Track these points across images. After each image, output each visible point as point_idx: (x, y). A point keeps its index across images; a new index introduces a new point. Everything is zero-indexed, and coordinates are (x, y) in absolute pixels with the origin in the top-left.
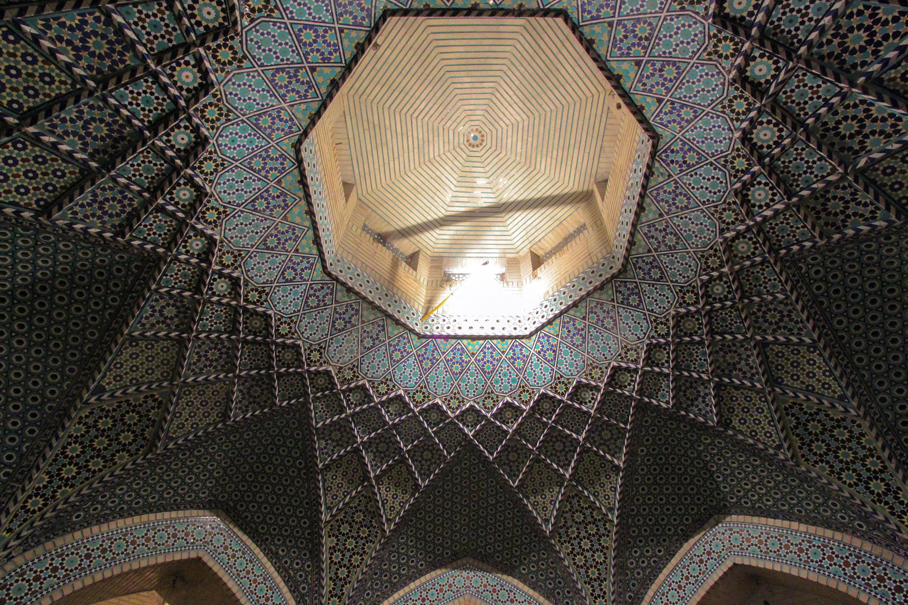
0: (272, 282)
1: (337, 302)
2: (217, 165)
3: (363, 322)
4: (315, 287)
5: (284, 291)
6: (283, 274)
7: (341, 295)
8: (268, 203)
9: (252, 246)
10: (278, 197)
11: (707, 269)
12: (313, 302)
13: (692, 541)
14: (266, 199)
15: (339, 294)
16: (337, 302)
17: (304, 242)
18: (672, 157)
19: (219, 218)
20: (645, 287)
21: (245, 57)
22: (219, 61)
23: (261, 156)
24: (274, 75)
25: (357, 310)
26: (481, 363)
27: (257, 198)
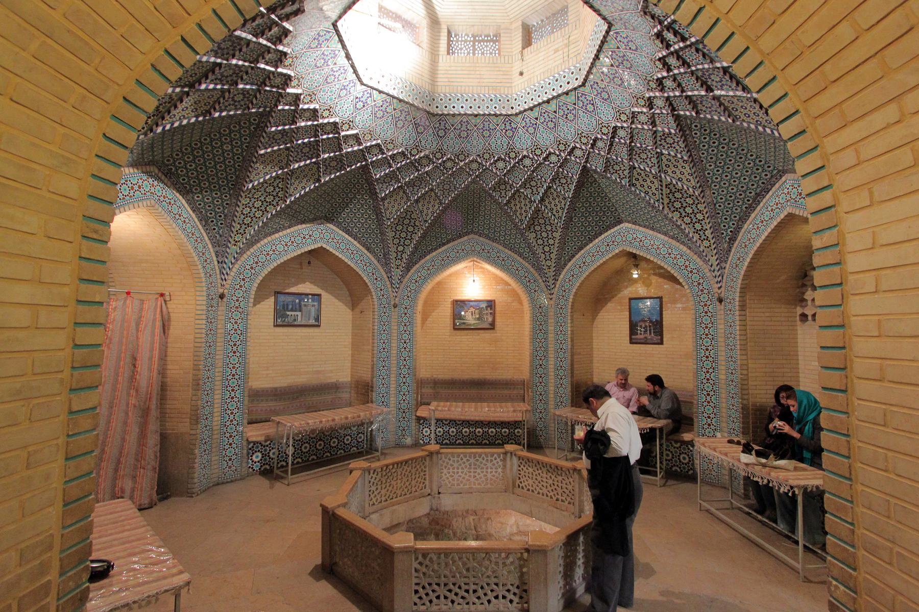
11: (457, 156)
13: (304, 226)
18: (508, 124)
20: (431, 131)
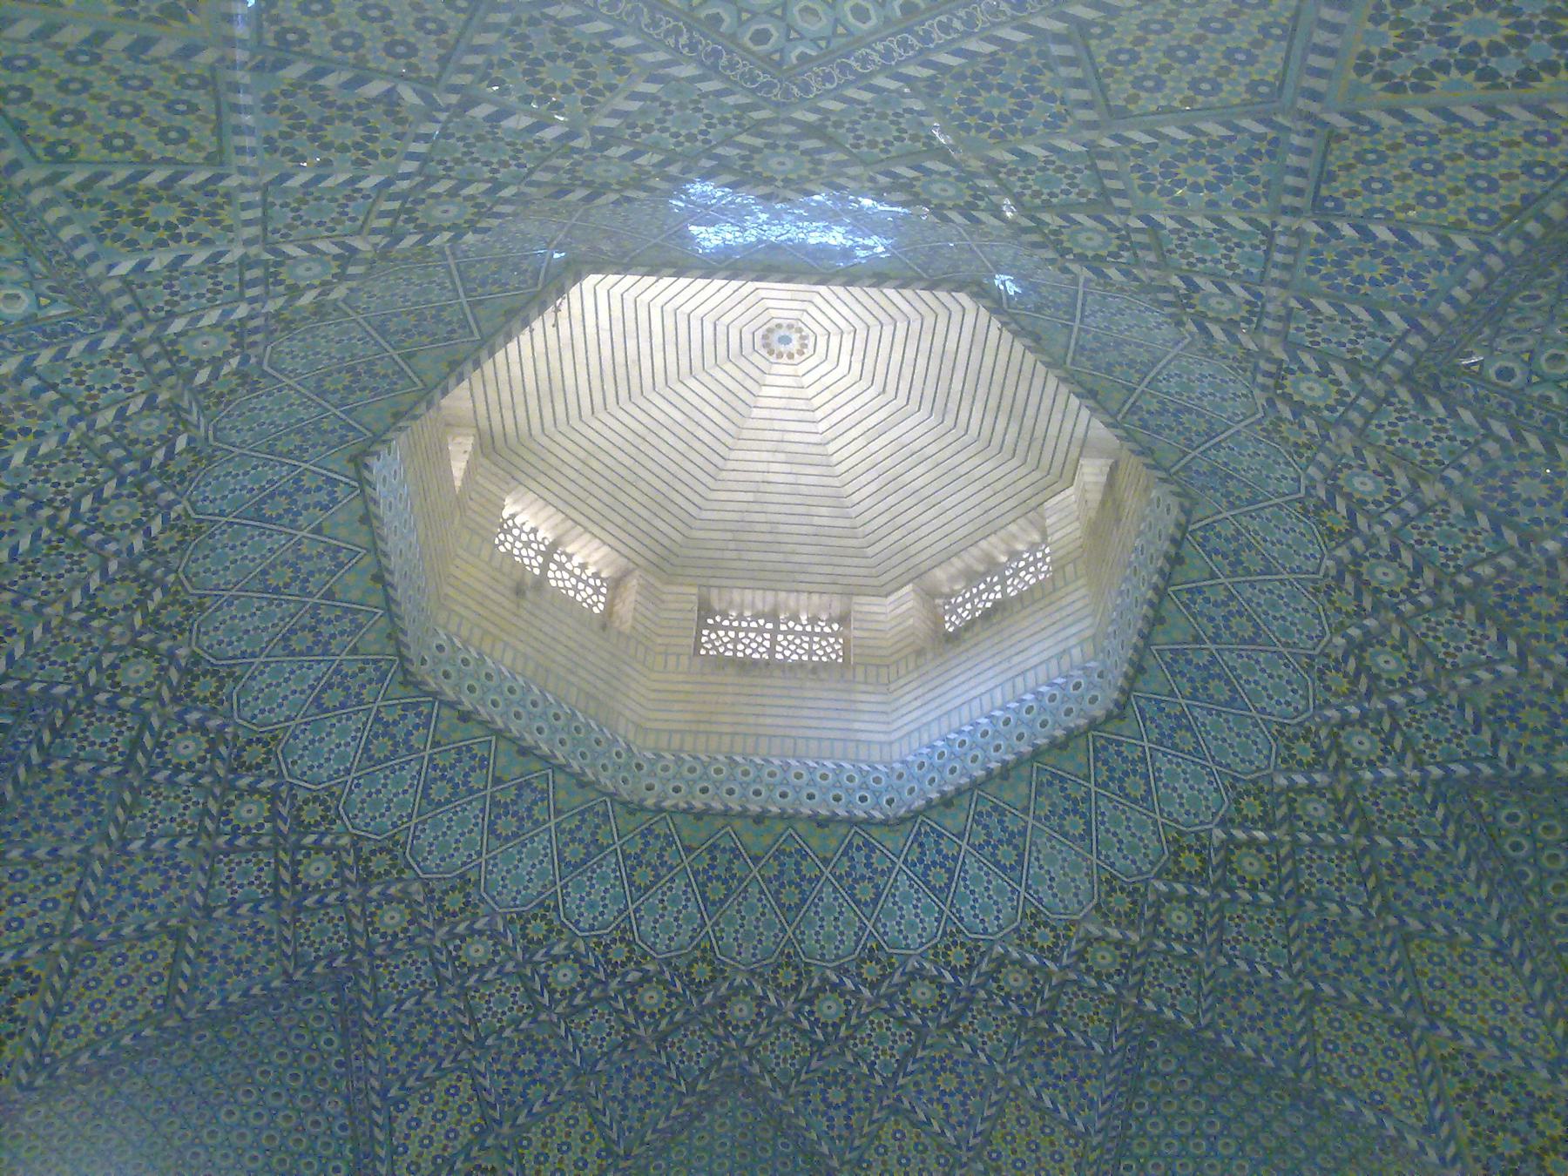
0: (863, 928)
1: (960, 836)
2: (622, 939)
3: (1025, 810)
4: (912, 857)
5: (890, 915)
6: (857, 903)
7: (953, 821)
8: (718, 878)
9: (783, 930)
10: (714, 858)
12: (938, 877)
14: (710, 879)
15: (948, 823)
16: (960, 836)
17: (814, 842)
19: (711, 963)
21: (462, 876)
22: (462, 910)
23: (633, 868)
24: (498, 837)
25: (995, 808)
26: (1226, 635)
27: (703, 894)
